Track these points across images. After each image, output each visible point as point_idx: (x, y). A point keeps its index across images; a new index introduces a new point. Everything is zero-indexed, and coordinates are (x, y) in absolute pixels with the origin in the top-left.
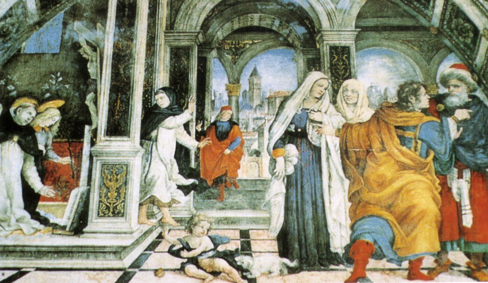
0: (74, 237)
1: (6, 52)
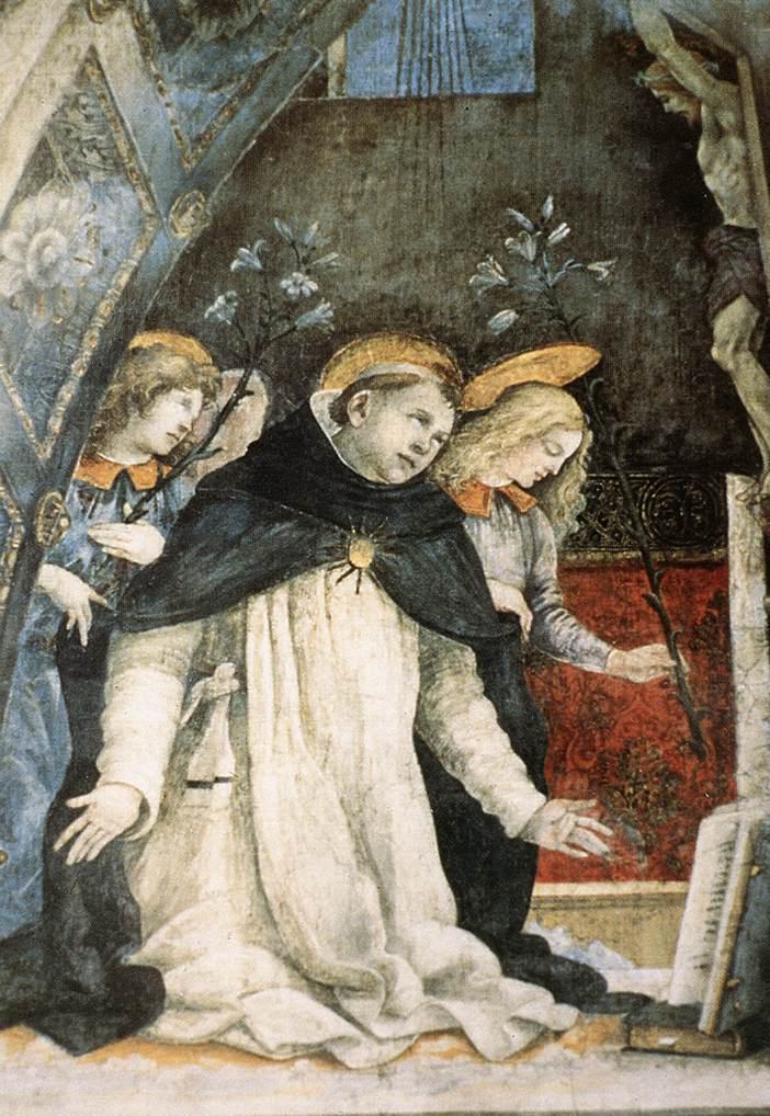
0: (748, 1065)
1: (243, 94)
